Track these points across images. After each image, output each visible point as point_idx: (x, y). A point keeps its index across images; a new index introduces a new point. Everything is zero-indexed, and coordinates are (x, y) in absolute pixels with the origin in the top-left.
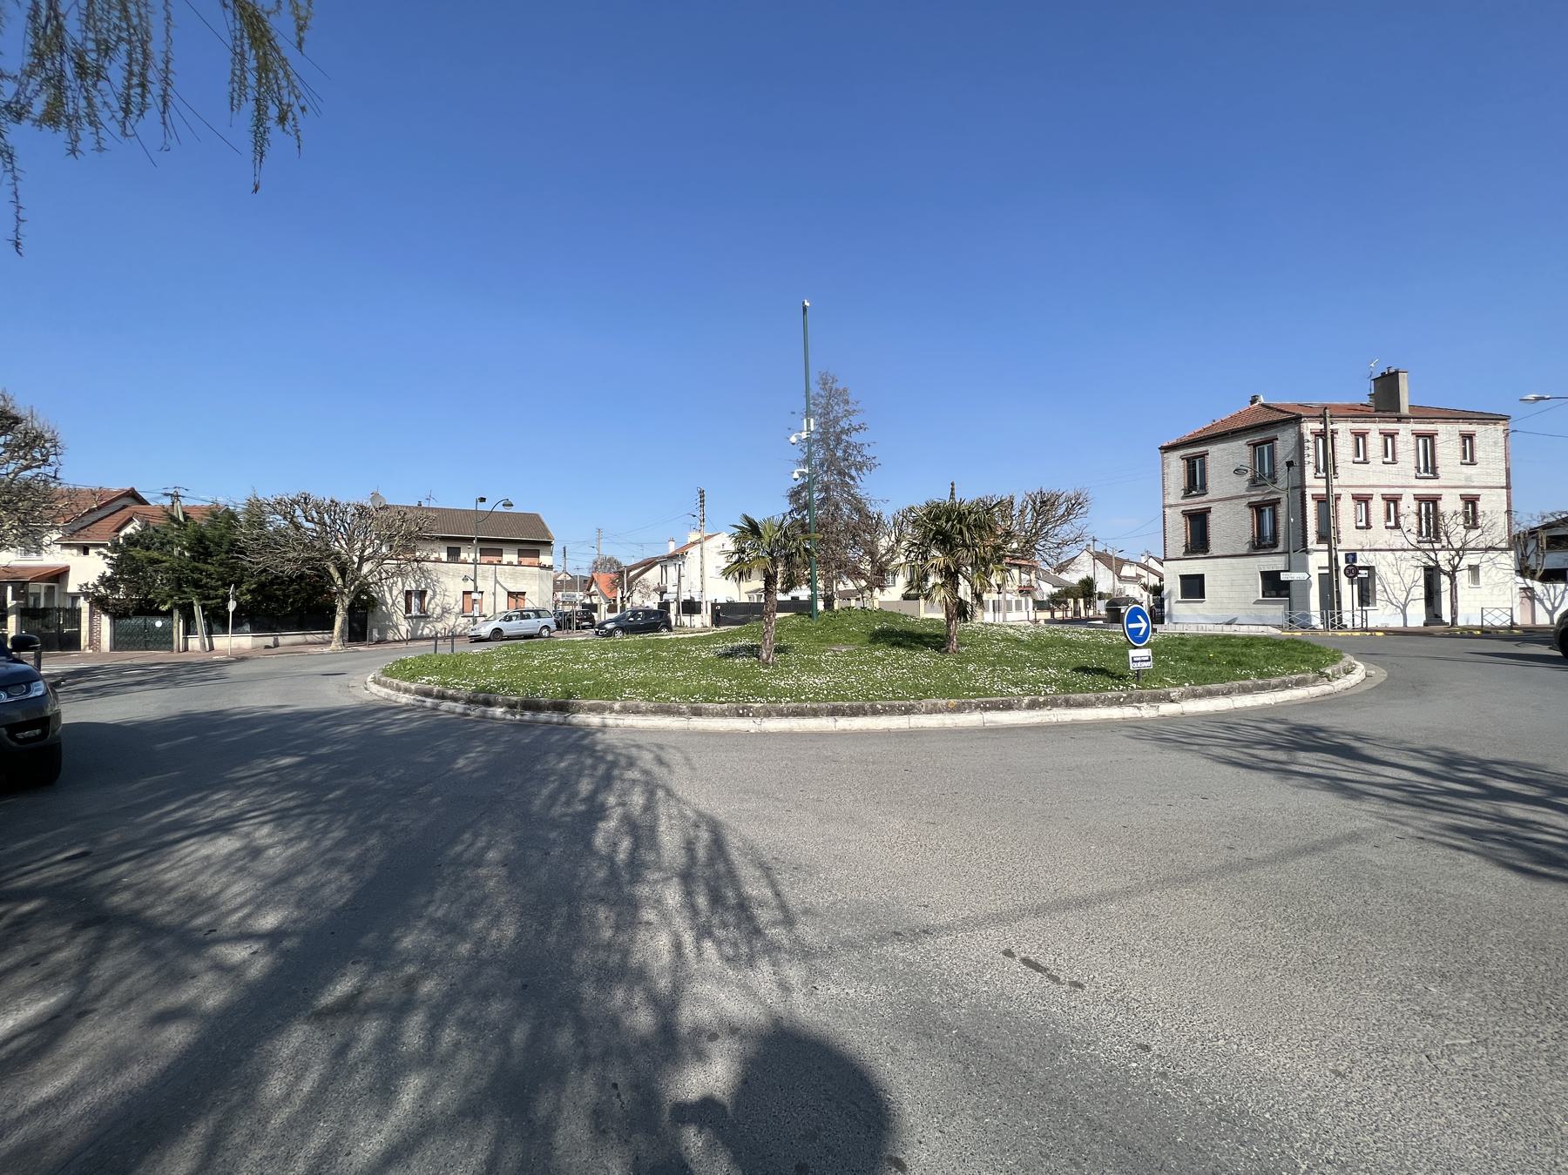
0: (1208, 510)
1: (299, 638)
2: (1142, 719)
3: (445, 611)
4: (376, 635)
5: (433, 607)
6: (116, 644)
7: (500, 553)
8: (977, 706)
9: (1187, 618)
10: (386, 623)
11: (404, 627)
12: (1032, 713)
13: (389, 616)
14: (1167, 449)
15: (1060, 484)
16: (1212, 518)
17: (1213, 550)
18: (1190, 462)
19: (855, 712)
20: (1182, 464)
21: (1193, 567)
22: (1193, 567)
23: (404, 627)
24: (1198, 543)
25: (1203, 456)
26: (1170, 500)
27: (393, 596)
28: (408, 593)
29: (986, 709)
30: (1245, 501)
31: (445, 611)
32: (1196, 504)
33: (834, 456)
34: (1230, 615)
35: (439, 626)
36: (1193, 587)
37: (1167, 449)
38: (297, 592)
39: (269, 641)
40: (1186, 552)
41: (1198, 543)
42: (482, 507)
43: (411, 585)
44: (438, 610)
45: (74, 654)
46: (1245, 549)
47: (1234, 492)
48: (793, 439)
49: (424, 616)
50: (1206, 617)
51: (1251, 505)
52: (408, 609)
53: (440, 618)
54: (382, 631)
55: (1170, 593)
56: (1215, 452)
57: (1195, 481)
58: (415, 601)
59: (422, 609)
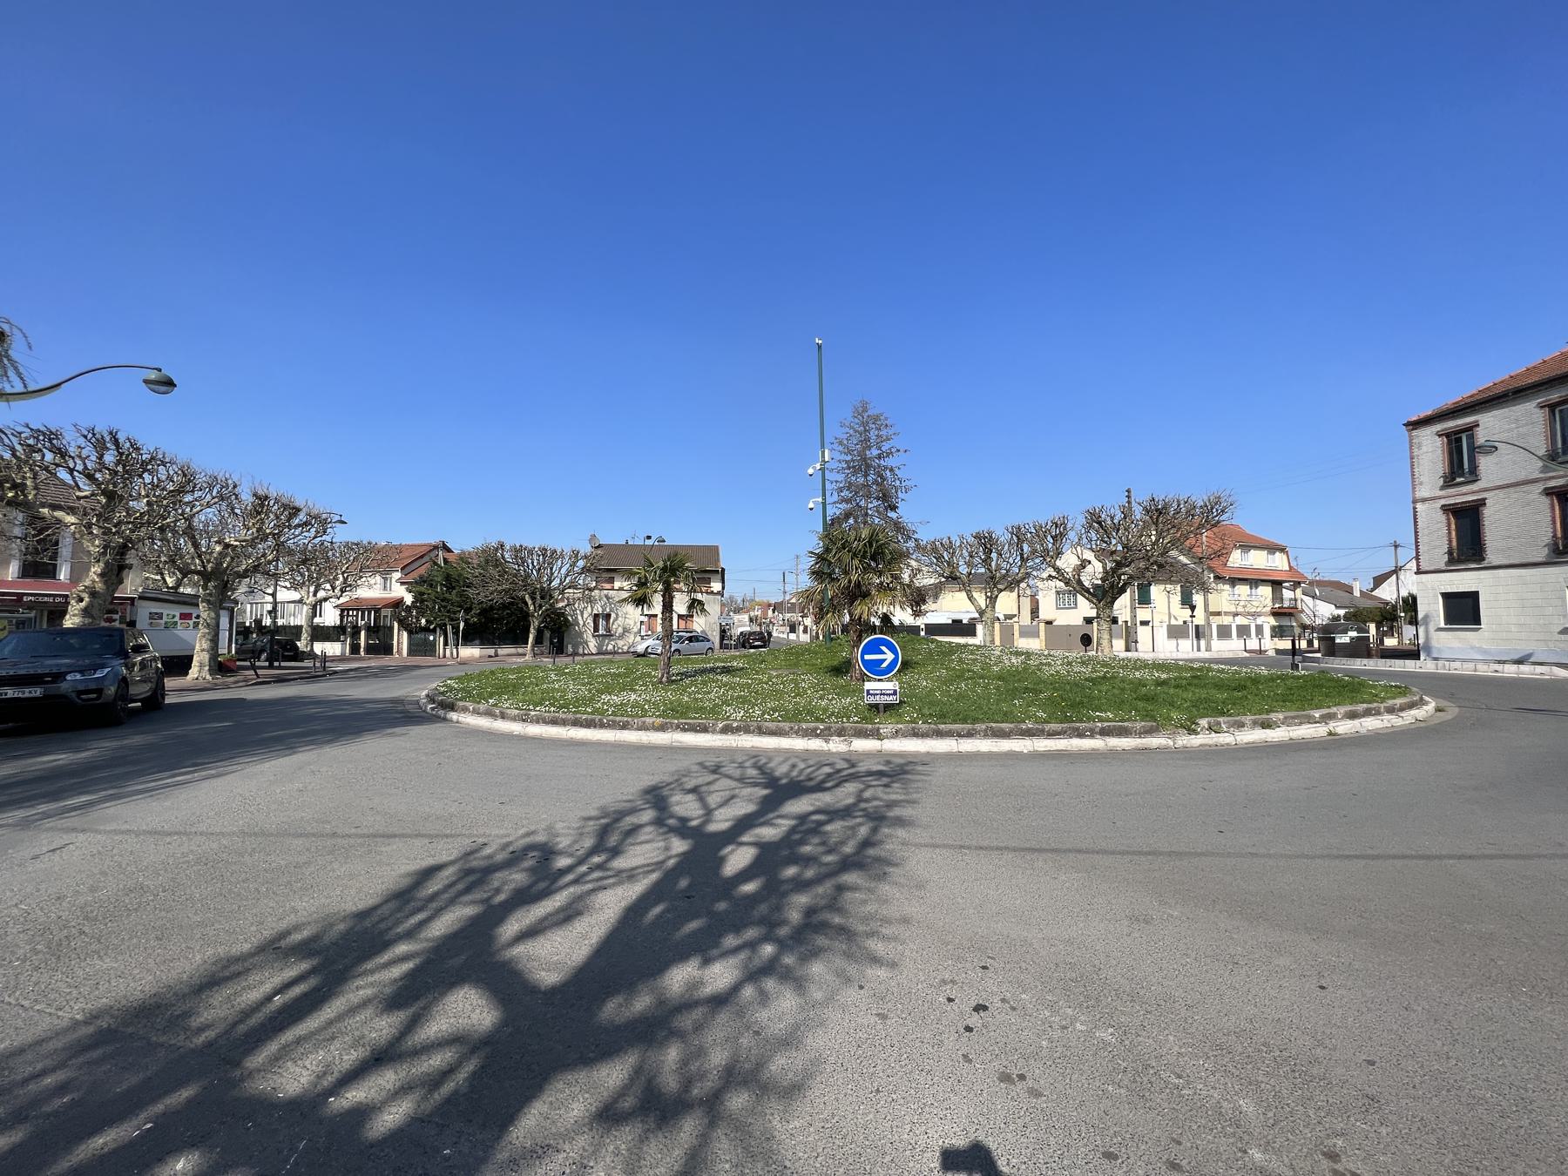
0: (1482, 503)
1: (513, 651)
2: (829, 753)
3: (626, 630)
4: (570, 649)
5: (616, 627)
6: (410, 653)
7: (611, 580)
8: (678, 727)
9: (1454, 651)
10: (579, 640)
11: (592, 645)
12: (724, 737)
13: (580, 634)
14: (1415, 425)
15: (1184, 486)
16: (1488, 513)
17: (1492, 557)
18: (1454, 441)
19: (589, 724)
20: (1440, 443)
21: (1462, 581)
22: (1462, 581)
23: (592, 645)
24: (1469, 542)
25: (1470, 429)
26: (1423, 492)
27: (583, 618)
28: (596, 617)
29: (684, 730)
30: (1540, 487)
31: (626, 630)
32: (1463, 495)
33: (870, 479)
34: (1522, 648)
35: (621, 643)
36: (1463, 609)
37: (1415, 425)
38: (510, 615)
39: (492, 652)
40: (1451, 561)
41: (1469, 542)
42: (649, 542)
43: (598, 609)
44: (620, 630)
45: (387, 658)
46: (1541, 554)
47: (1522, 476)
48: (811, 471)
49: (609, 634)
50: (1485, 652)
51: (1548, 492)
52: (596, 629)
53: (621, 637)
54: (575, 646)
55: (1426, 617)
56: (1490, 425)
57: (1461, 459)
58: (602, 622)
59: (608, 629)
